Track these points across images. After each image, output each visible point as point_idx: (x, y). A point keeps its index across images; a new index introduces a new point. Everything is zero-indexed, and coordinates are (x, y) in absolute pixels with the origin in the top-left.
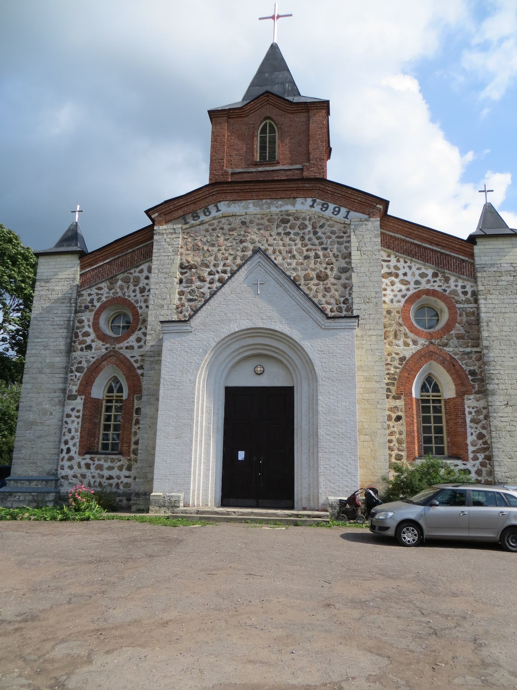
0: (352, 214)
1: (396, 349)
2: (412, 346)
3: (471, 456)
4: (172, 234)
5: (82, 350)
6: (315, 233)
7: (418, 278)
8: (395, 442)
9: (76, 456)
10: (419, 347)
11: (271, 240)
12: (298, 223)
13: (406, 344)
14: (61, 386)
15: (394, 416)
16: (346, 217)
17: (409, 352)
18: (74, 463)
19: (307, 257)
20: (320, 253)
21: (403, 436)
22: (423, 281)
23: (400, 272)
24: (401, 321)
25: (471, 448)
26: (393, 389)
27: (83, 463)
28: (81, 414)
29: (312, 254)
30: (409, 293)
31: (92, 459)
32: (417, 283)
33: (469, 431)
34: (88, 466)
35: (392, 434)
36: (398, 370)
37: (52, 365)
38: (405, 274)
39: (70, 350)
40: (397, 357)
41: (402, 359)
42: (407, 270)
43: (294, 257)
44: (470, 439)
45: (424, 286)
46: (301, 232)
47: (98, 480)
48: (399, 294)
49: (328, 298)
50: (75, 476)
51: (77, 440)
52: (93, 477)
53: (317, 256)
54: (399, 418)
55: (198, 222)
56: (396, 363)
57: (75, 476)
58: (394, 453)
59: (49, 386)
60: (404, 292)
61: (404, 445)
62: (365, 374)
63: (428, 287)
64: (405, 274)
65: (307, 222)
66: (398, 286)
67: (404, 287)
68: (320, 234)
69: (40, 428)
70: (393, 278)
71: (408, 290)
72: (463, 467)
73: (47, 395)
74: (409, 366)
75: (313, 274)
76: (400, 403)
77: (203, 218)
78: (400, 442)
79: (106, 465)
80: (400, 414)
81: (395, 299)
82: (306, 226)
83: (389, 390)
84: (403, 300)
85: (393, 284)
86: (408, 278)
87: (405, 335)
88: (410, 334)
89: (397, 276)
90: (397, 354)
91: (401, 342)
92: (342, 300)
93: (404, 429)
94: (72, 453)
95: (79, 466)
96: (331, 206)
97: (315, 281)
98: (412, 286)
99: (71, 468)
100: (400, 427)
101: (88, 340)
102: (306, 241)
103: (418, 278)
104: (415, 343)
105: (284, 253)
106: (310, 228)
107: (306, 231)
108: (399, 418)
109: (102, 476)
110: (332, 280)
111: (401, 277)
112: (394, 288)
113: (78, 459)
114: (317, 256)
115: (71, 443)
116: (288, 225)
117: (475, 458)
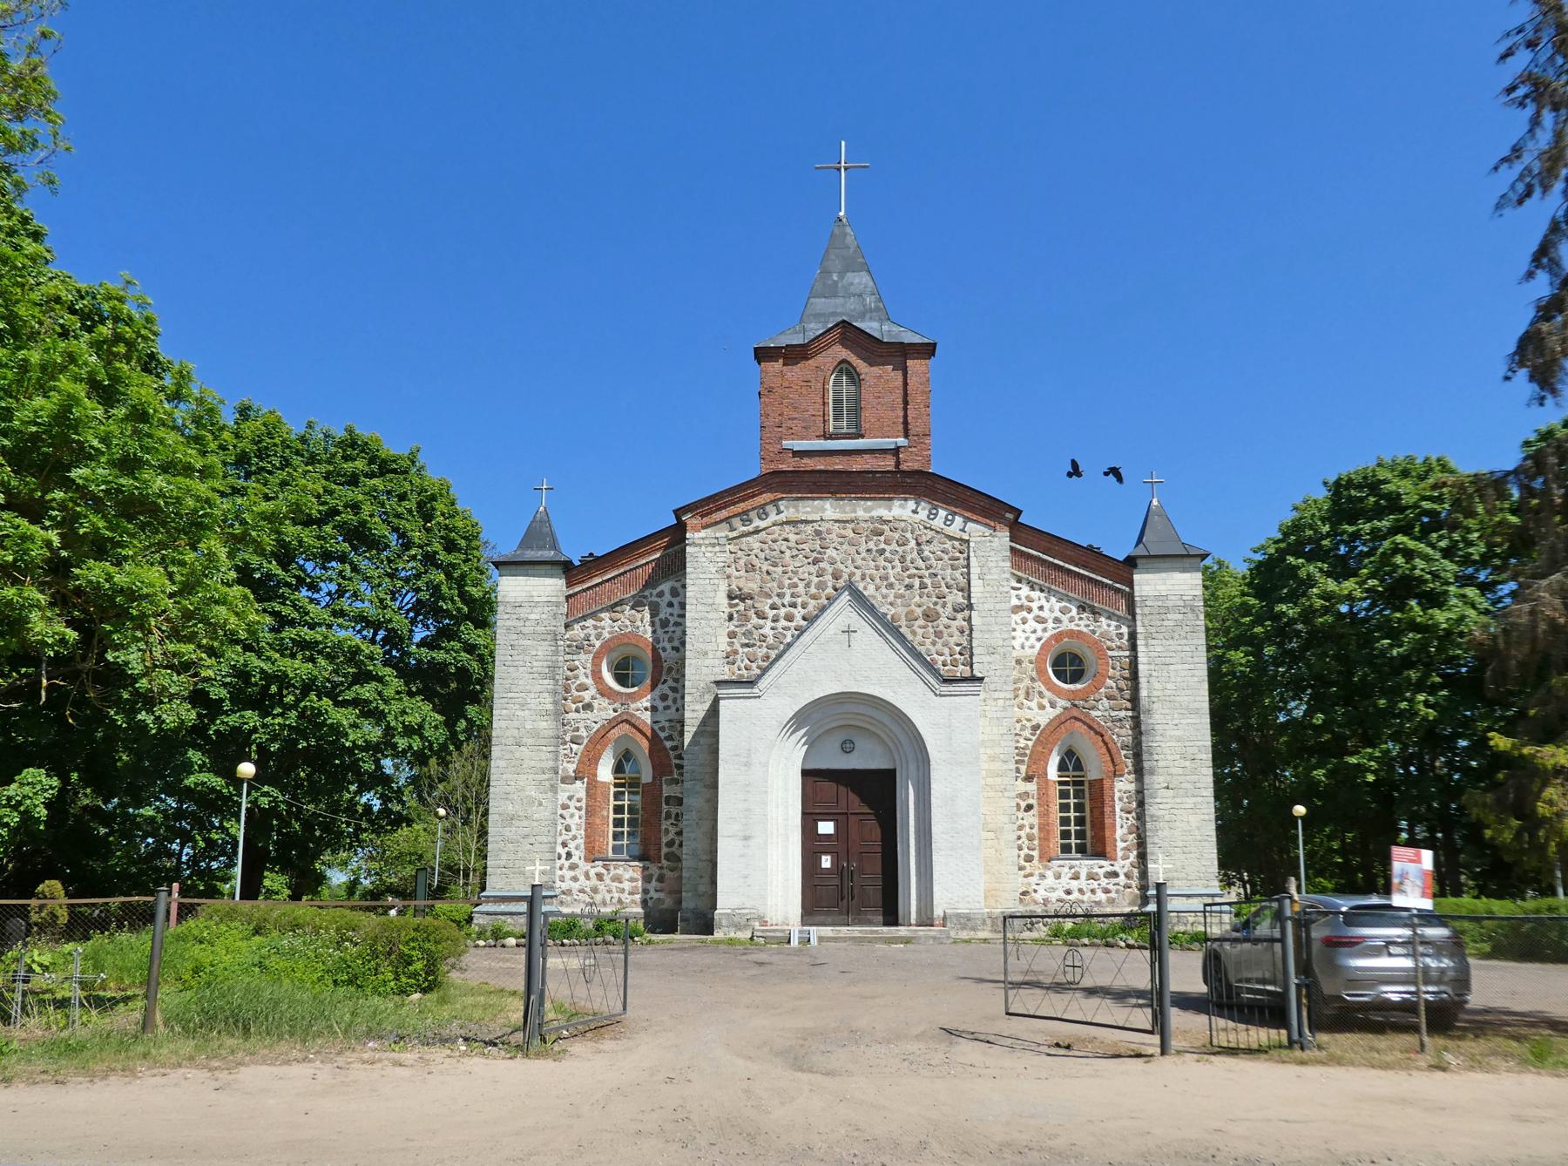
0: (970, 525)
1: (1029, 714)
3: (1120, 854)
4: (713, 545)
5: (577, 711)
7: (1059, 614)
8: (1024, 839)
9: (582, 863)
10: (1058, 711)
12: (896, 535)
14: (551, 764)
15: (1023, 805)
16: (963, 530)
17: (1044, 717)
18: (578, 873)
19: (909, 587)
20: (928, 581)
21: (1035, 831)
22: (1065, 618)
23: (1035, 605)
24: (1034, 674)
25: (1120, 845)
26: (1023, 768)
27: (592, 873)
28: (583, 804)
29: (917, 582)
30: (1047, 635)
31: (604, 866)
32: (1057, 620)
34: (600, 877)
35: (1021, 828)
36: (1030, 743)
37: (535, 733)
38: (1041, 608)
39: (559, 713)
40: (1029, 724)
41: (1036, 728)
42: (1043, 602)
43: (891, 586)
44: (1119, 833)
45: (1066, 625)
47: (616, 895)
48: (1033, 637)
49: (939, 646)
50: (582, 891)
51: (581, 841)
52: (609, 891)
53: (923, 586)
54: (1029, 808)
55: (750, 528)
56: (1027, 733)
57: (582, 891)
58: (1022, 853)
59: (533, 763)
60: (1039, 633)
61: (1036, 842)
62: (989, 751)
63: (1072, 626)
65: (909, 535)
66: (1032, 624)
67: (1039, 627)
68: (926, 553)
69: (525, 823)
70: (1024, 613)
71: (1045, 630)
72: (1109, 869)
73: (531, 777)
74: (1045, 736)
75: (919, 611)
76: (1032, 787)
77: (758, 523)
78: (1030, 838)
79: (627, 876)
80: (1031, 801)
81: (1027, 644)
83: (1018, 770)
84: (1038, 645)
85: (1024, 621)
86: (1045, 614)
87: (1040, 693)
88: (1048, 694)
89: (1030, 610)
91: (1034, 704)
92: (958, 649)
93: (1035, 821)
94: (575, 859)
95: (587, 877)
96: (942, 513)
97: (921, 622)
98: (1050, 625)
99: (575, 879)
100: (1031, 818)
101: (587, 696)
103: (1059, 614)
104: (1053, 705)
105: (878, 581)
106: (913, 543)
107: (908, 548)
108: (1029, 808)
109: (623, 891)
110: (944, 620)
111: (1036, 612)
112: (1026, 627)
113: (584, 866)
114: (923, 586)
115: (572, 845)
116: (882, 538)
117: (1125, 858)
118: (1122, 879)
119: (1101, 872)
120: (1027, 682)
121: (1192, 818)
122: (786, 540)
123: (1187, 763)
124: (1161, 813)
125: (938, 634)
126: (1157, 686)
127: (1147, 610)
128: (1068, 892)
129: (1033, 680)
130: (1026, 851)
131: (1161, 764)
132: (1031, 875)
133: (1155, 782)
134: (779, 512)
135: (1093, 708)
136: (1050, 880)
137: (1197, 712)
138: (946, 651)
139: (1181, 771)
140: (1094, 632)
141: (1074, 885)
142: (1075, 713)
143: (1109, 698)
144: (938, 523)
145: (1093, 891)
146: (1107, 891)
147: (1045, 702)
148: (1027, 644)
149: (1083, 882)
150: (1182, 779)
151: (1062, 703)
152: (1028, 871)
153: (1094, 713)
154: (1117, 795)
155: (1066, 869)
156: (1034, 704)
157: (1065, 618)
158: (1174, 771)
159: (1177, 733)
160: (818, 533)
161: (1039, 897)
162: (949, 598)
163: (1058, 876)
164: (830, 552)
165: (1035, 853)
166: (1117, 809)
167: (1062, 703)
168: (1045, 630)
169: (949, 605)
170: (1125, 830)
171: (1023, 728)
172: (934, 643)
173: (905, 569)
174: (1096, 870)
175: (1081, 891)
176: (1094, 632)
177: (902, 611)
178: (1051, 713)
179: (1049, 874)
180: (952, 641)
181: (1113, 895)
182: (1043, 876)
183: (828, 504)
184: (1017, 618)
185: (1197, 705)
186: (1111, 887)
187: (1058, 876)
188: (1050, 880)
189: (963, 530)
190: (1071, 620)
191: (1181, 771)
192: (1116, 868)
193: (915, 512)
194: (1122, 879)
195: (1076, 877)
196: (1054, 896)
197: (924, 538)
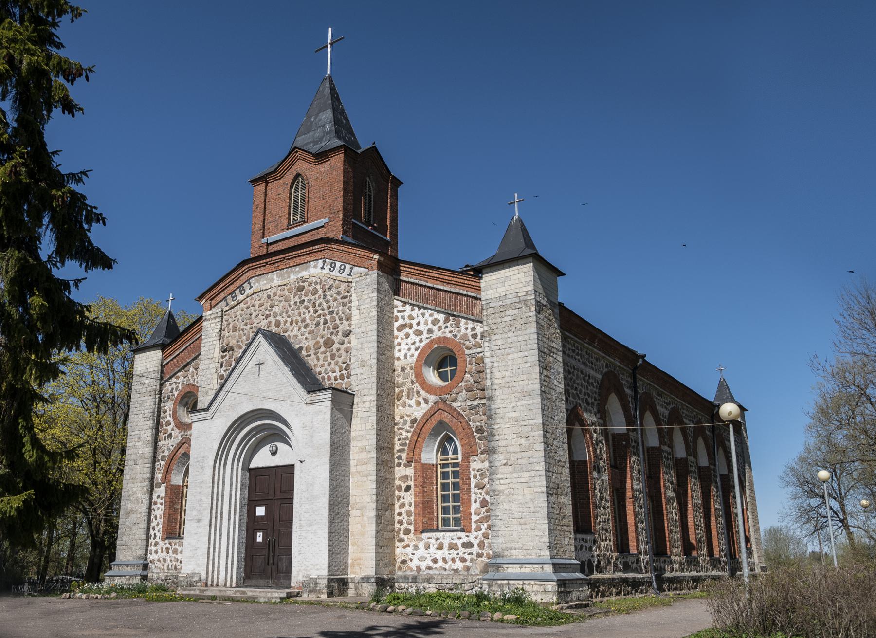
1: (408, 411)
2: (423, 405)
3: (474, 526)
6: (325, 296)
7: (430, 326)
8: (404, 515)
10: (430, 404)
11: (290, 313)
13: (418, 404)
15: (404, 486)
20: (328, 318)
21: (412, 508)
22: (435, 328)
23: (414, 322)
25: (474, 518)
30: (422, 345)
33: (473, 496)
36: (409, 434)
38: (419, 324)
40: (409, 419)
41: (414, 421)
42: (420, 318)
43: (306, 326)
44: (474, 506)
45: (437, 334)
46: (313, 298)
48: (413, 347)
49: (332, 366)
53: (325, 322)
54: (408, 488)
56: (407, 427)
60: (417, 344)
61: (412, 518)
64: (419, 324)
65: (318, 287)
66: (413, 337)
67: (417, 339)
68: (328, 297)
70: (407, 330)
71: (421, 341)
72: (465, 540)
75: (322, 341)
78: (409, 514)
81: (409, 354)
82: (317, 290)
84: (416, 354)
85: (407, 336)
87: (418, 392)
88: (422, 392)
89: (411, 327)
90: (409, 416)
91: (413, 402)
97: (323, 349)
98: (425, 335)
102: (317, 307)
103: (430, 326)
105: (300, 323)
107: (317, 296)
110: (336, 345)
111: (415, 327)
112: (409, 341)
114: (325, 322)
116: (303, 292)
117: (478, 529)
118: (475, 549)
119: (459, 542)
120: (409, 385)
121: (526, 491)
122: (253, 306)
123: (523, 441)
124: (501, 488)
125: (333, 356)
126: (497, 374)
127: (490, 311)
128: (435, 561)
129: (412, 382)
130: (405, 525)
131: (501, 443)
132: (408, 546)
133: (500, 458)
134: (251, 287)
135: (455, 400)
136: (422, 551)
137: (528, 394)
138: (337, 369)
139: (517, 449)
140: (455, 336)
141: (439, 554)
142: (441, 406)
143: (469, 389)
144: (336, 273)
145: (453, 560)
146: (463, 560)
147: (421, 400)
148: (409, 354)
149: (445, 553)
150: (518, 455)
151: (432, 398)
152: (406, 542)
153: (455, 405)
154: (472, 473)
155: (433, 541)
156: (413, 402)
157: (435, 328)
158: (511, 449)
159: (514, 415)
160: (269, 297)
161: (413, 565)
162: (341, 327)
163: (427, 547)
164: (276, 309)
165: (412, 527)
166: (473, 486)
167: (432, 398)
168: (421, 341)
169: (340, 333)
170: (478, 505)
171: (405, 422)
172: (329, 364)
173: (316, 312)
174: (456, 541)
175: (444, 560)
176: (455, 336)
177: (311, 343)
178: (425, 408)
179: (421, 545)
180: (340, 360)
181: (468, 564)
182: (416, 547)
183: (274, 275)
184: (402, 334)
185: (530, 388)
186: (466, 556)
187: (427, 547)
188: (422, 551)
189: (350, 275)
190: (440, 329)
191: (517, 449)
192: (472, 539)
193: (323, 268)
194: (475, 549)
195: (440, 547)
196: (423, 565)
197: (327, 287)
